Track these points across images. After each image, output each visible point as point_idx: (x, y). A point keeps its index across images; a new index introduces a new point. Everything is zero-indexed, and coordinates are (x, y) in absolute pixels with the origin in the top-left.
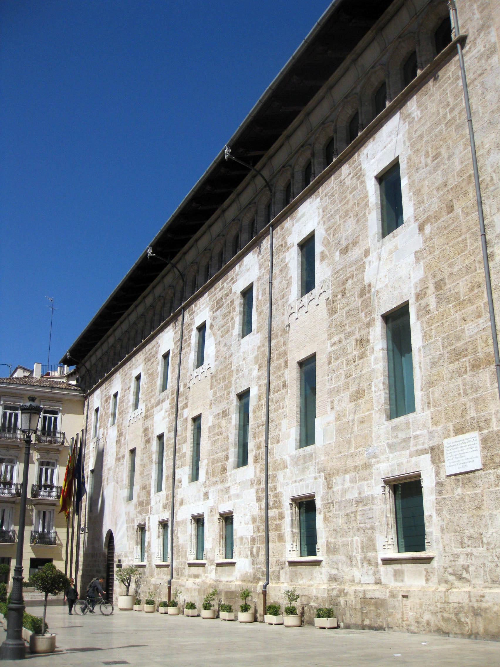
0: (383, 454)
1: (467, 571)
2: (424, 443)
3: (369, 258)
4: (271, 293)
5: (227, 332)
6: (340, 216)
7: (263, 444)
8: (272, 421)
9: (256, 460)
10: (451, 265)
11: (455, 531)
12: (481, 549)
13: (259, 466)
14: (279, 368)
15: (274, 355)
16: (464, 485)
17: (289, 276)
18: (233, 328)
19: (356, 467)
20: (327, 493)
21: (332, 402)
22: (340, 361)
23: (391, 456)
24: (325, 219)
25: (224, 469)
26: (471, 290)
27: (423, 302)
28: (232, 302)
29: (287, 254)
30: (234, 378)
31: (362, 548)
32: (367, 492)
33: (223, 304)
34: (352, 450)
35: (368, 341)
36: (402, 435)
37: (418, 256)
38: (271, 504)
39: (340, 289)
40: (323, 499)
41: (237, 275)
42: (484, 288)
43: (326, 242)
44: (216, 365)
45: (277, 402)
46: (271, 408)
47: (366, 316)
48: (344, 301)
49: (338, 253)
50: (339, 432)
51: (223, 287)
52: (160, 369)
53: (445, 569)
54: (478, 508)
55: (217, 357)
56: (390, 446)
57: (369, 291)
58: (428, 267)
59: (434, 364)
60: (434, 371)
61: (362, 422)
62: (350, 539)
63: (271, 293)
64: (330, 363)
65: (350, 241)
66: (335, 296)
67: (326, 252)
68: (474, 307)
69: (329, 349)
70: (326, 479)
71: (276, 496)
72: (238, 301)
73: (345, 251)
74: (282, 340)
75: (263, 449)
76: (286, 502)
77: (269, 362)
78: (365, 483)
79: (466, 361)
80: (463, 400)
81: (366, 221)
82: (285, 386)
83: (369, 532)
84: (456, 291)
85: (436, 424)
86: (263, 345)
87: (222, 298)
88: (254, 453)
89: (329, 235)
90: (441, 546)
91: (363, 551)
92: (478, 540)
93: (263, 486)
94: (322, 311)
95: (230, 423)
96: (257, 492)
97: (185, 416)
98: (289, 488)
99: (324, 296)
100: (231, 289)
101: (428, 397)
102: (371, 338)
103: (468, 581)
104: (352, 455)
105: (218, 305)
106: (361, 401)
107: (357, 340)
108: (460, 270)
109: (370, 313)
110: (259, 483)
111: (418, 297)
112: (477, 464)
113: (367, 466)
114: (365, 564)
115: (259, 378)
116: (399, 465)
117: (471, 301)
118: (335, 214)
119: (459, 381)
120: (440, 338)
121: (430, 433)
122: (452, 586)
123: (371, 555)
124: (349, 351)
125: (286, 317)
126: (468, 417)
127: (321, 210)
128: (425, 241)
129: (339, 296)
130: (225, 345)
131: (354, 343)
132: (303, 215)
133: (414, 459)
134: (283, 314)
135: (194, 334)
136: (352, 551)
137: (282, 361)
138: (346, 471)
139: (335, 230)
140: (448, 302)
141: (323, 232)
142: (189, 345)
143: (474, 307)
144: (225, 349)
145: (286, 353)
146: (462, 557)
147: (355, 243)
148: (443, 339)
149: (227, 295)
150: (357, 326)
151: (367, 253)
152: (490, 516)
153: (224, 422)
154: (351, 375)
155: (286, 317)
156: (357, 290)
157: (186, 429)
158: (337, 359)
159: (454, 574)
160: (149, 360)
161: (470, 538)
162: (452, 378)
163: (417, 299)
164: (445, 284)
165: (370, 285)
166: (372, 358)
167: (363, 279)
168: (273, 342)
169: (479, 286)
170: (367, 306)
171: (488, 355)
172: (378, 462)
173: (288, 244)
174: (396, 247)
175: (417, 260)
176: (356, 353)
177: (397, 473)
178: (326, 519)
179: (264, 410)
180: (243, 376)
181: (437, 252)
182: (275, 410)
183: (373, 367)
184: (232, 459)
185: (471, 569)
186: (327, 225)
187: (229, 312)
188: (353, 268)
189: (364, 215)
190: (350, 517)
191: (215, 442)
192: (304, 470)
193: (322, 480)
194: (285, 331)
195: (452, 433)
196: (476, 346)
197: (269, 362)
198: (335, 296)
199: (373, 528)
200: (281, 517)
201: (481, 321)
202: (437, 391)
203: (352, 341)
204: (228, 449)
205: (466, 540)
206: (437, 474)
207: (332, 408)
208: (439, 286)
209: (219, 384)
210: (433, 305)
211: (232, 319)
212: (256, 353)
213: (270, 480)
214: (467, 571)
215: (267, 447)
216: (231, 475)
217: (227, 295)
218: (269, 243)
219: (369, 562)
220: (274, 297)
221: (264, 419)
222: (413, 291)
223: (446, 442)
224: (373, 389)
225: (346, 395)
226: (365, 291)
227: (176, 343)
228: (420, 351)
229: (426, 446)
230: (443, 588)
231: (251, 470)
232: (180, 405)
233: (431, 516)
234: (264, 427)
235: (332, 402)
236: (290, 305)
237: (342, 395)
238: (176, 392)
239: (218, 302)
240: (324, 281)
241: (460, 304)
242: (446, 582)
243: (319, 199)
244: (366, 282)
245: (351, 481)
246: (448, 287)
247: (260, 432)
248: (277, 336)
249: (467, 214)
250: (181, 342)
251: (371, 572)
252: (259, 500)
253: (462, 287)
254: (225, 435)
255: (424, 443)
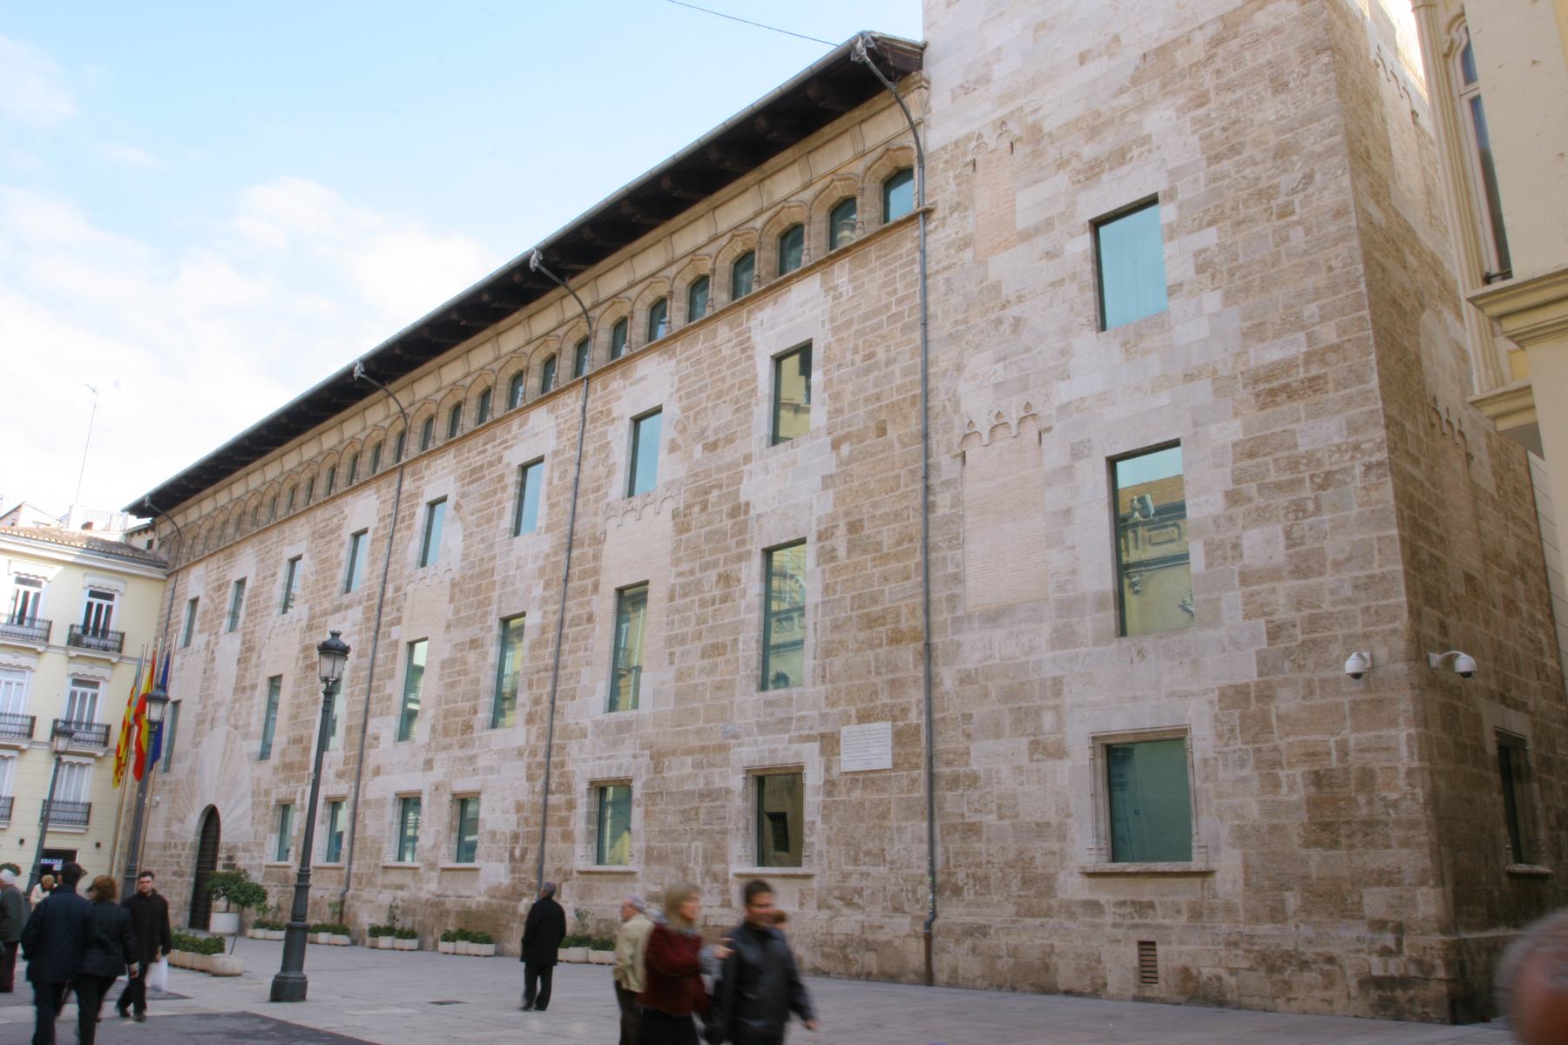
0: (748, 735)
1: (860, 896)
2: (811, 728)
3: (749, 467)
4: (577, 479)
5: (488, 521)
6: (708, 397)
7: (545, 699)
8: (565, 667)
9: (530, 719)
10: (875, 505)
11: (847, 844)
12: (882, 869)
13: (534, 730)
14: (583, 592)
15: (575, 570)
16: (865, 787)
17: (611, 461)
18: (500, 516)
19: (703, 749)
20: (653, 779)
21: (672, 654)
22: (688, 599)
23: (761, 738)
24: (682, 393)
25: (468, 727)
26: (899, 543)
27: (828, 544)
28: (501, 477)
29: (610, 428)
30: (497, 593)
31: (705, 857)
32: (718, 783)
33: (483, 477)
34: (701, 725)
35: (739, 580)
36: (779, 713)
37: (827, 482)
38: (553, 787)
39: (699, 499)
40: (645, 786)
41: (515, 437)
42: (918, 544)
43: (680, 427)
44: (463, 569)
45: (576, 640)
46: (566, 647)
47: (738, 545)
48: (704, 517)
49: (699, 448)
50: (681, 697)
51: (484, 451)
52: (345, 555)
53: (829, 891)
54: (883, 816)
55: (465, 557)
56: (759, 725)
57: (747, 512)
58: (840, 499)
59: (836, 627)
60: (836, 637)
61: (718, 688)
62: (685, 845)
63: (577, 479)
64: (671, 599)
65: (721, 435)
66: (689, 507)
67: (680, 440)
68: (901, 565)
69: (673, 580)
70: (652, 758)
71: (562, 775)
72: (512, 479)
73: (712, 447)
74: (590, 551)
75: (545, 704)
76: (581, 788)
77: (566, 581)
78: (717, 771)
79: (883, 631)
80: (873, 679)
81: (751, 414)
82: (590, 619)
83: (718, 837)
84: (878, 538)
85: (832, 704)
86: (556, 554)
87: (482, 466)
88: (527, 709)
89: (687, 418)
90: (825, 861)
91: (705, 863)
92: (879, 857)
93: (541, 758)
94: (665, 524)
95: (484, 659)
96: (529, 766)
97: (394, 637)
98: (586, 764)
99: (670, 506)
100: (500, 459)
101: (824, 669)
102: (743, 576)
103: (859, 907)
104: (698, 732)
105: (475, 474)
106: (720, 659)
107: (720, 576)
108: (887, 514)
109: (743, 542)
110: (533, 753)
111: (821, 536)
112: (886, 763)
113: (722, 748)
114: (707, 880)
115: (545, 601)
116: (772, 752)
117: (897, 557)
118: (701, 390)
119: (870, 655)
120: (848, 596)
121: (824, 717)
122: (838, 914)
123: (717, 867)
124: (706, 588)
125: (599, 519)
126: (878, 703)
127: (676, 379)
128: (840, 464)
129: (697, 509)
130: (483, 540)
131: (714, 578)
132: (643, 378)
133: (795, 747)
134: (596, 514)
135: (421, 512)
136: (689, 860)
137: (589, 582)
138: (689, 752)
139: (697, 413)
140: (865, 552)
141: (678, 412)
142: (410, 527)
143: (901, 565)
144: (482, 546)
145: (596, 572)
146: (854, 877)
147: (730, 440)
148: (853, 597)
149: (491, 464)
150: (722, 556)
151: (747, 459)
152: (899, 828)
153: (472, 657)
154: (705, 622)
155: (599, 519)
156: (726, 507)
157: (394, 657)
158: (685, 595)
159: (841, 898)
160: (322, 537)
161: (868, 853)
162: (859, 650)
163: (820, 538)
164: (862, 527)
165: (747, 505)
166: (743, 603)
167: (737, 492)
168: (575, 553)
169: (911, 540)
170: (741, 532)
171: (914, 629)
172: (739, 745)
173: (614, 414)
174: (794, 462)
175: (825, 487)
176: (717, 592)
177: (767, 763)
178: (647, 814)
179: (552, 649)
180: (514, 593)
181: (856, 483)
182: (571, 652)
183: (742, 616)
184: (485, 714)
185: (867, 892)
186: (685, 402)
187: (495, 492)
188: (724, 476)
189: (748, 405)
190: (687, 816)
191: (453, 685)
192: (614, 744)
193: (645, 761)
194: (598, 541)
195: (854, 719)
196: (898, 616)
197: (566, 581)
198: (689, 507)
199: (724, 832)
200: (571, 805)
201: (908, 584)
202: (837, 664)
203: (713, 574)
204: (477, 698)
205: (861, 856)
206: (828, 769)
207: (672, 663)
208: (854, 527)
209: (467, 597)
210: (842, 552)
211: (499, 503)
212: (541, 563)
213: (554, 752)
214: (860, 896)
215: (553, 703)
216: (480, 738)
217: (491, 464)
218: (581, 403)
219: (715, 877)
220: (582, 487)
221: (551, 661)
222: (815, 528)
223: (844, 730)
224: (741, 646)
225: (696, 647)
226: (739, 510)
227: (382, 520)
228: (816, 606)
229: (815, 732)
230: (824, 915)
231: (517, 732)
232: (384, 619)
233: (814, 823)
234: (551, 674)
235: (672, 654)
236: (608, 504)
237: (688, 647)
238: (378, 595)
239: (473, 472)
240: (672, 482)
241: (885, 558)
242: (829, 907)
243: (674, 362)
244: (743, 499)
245: (696, 765)
246: (866, 532)
247: (539, 680)
248: (582, 544)
249: (904, 445)
250: (395, 519)
251: (715, 891)
252: (530, 778)
253: (887, 536)
254: (472, 675)
255: (811, 728)
